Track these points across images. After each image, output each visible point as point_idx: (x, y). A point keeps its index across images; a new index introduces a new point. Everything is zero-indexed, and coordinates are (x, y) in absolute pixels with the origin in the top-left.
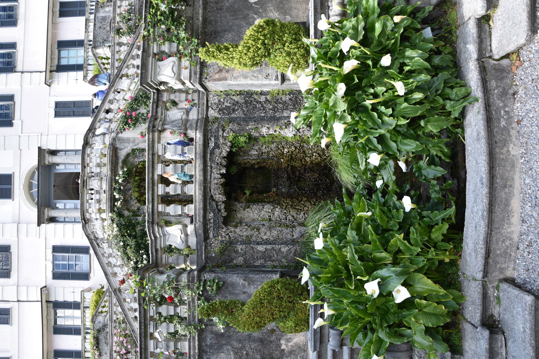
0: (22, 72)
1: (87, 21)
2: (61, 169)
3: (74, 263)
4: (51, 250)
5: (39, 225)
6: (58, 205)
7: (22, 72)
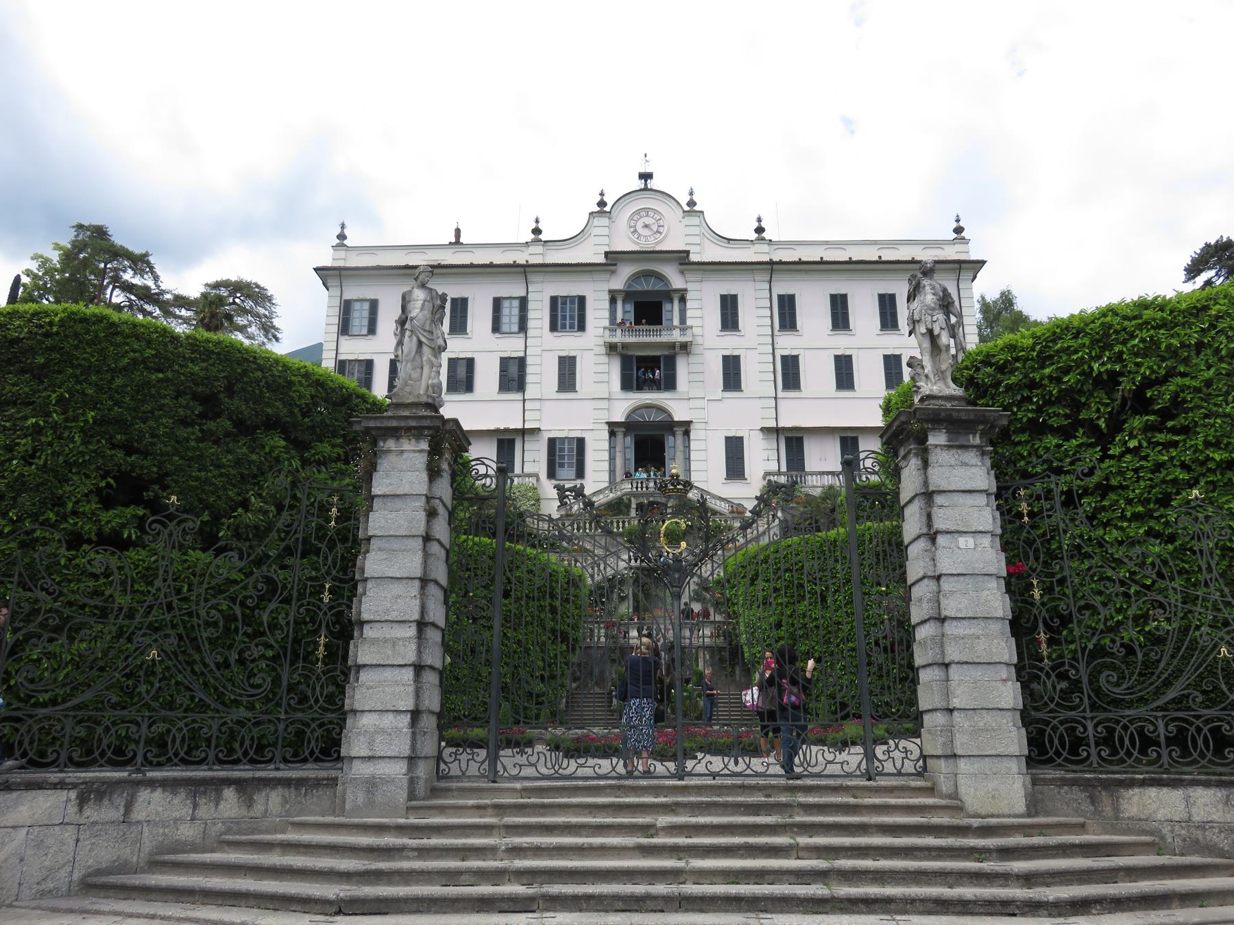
0: (776, 398)
1: (833, 473)
2: (669, 441)
3: (566, 461)
4: (579, 436)
5: (607, 423)
6: (628, 439)
7: (776, 398)
